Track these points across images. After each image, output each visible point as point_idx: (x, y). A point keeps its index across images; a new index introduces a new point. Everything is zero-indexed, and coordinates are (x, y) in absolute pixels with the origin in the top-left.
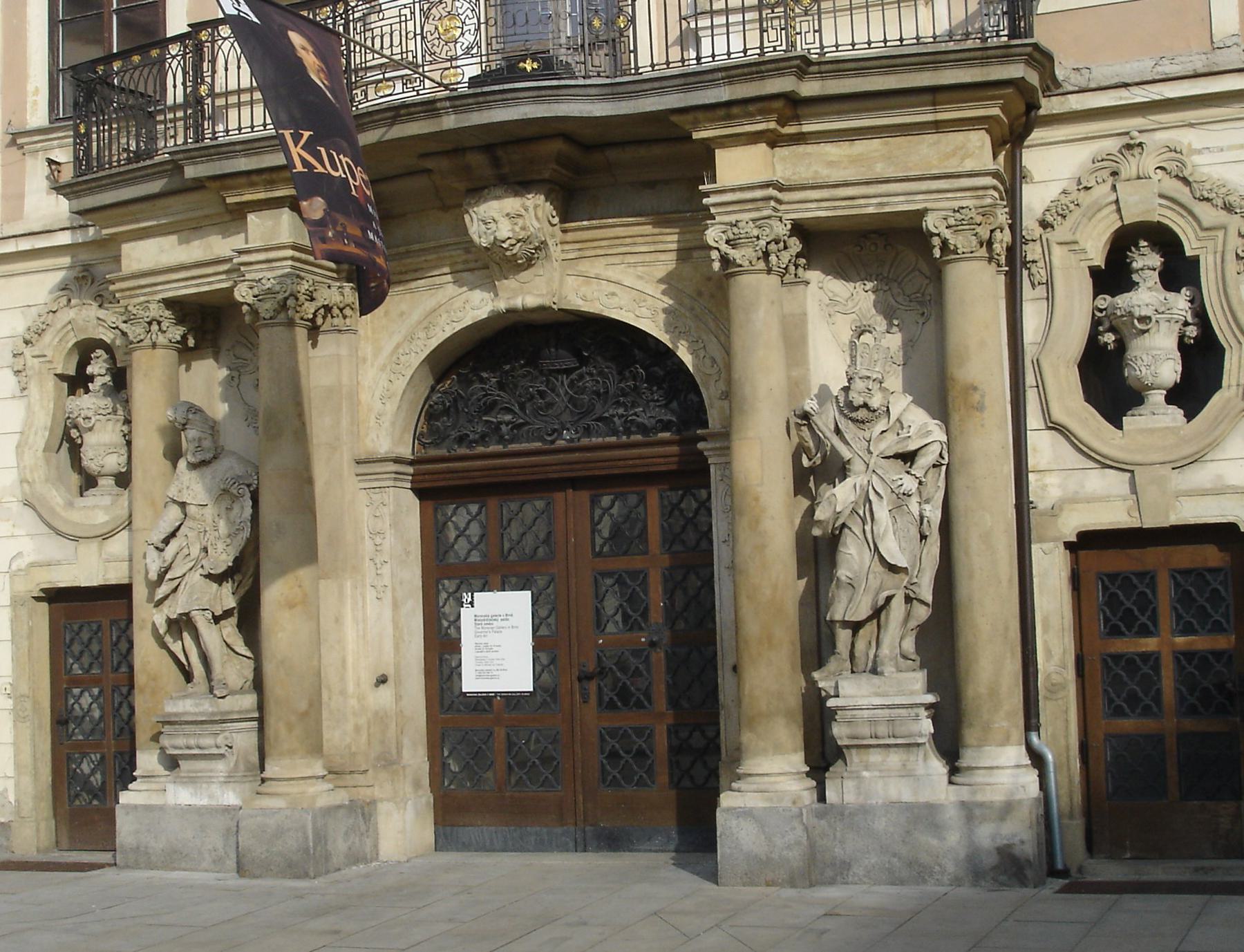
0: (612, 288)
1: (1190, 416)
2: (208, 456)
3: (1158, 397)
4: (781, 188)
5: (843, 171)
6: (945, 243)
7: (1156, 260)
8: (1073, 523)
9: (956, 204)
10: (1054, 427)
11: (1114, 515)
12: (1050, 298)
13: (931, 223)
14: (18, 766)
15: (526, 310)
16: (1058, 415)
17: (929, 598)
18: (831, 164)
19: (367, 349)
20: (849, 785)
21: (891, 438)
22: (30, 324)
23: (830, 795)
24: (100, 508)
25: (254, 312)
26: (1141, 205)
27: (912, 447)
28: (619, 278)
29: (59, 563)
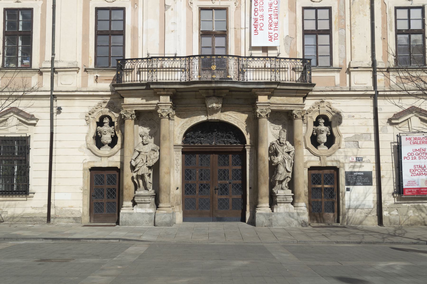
0: (230, 117)
1: (328, 149)
2: (147, 143)
3: (323, 144)
4: (271, 104)
5: (280, 102)
6: (296, 116)
7: (323, 121)
9: (299, 109)
10: (307, 148)
12: (307, 126)
13: (294, 112)
14: (83, 205)
15: (214, 120)
16: (308, 146)
17: (291, 177)
18: (277, 100)
19: (176, 124)
20: (278, 209)
21: (287, 149)
22: (90, 110)
23: (275, 210)
24: (106, 150)
25: (162, 116)
26: (323, 112)
27: (290, 150)
29: (96, 162)
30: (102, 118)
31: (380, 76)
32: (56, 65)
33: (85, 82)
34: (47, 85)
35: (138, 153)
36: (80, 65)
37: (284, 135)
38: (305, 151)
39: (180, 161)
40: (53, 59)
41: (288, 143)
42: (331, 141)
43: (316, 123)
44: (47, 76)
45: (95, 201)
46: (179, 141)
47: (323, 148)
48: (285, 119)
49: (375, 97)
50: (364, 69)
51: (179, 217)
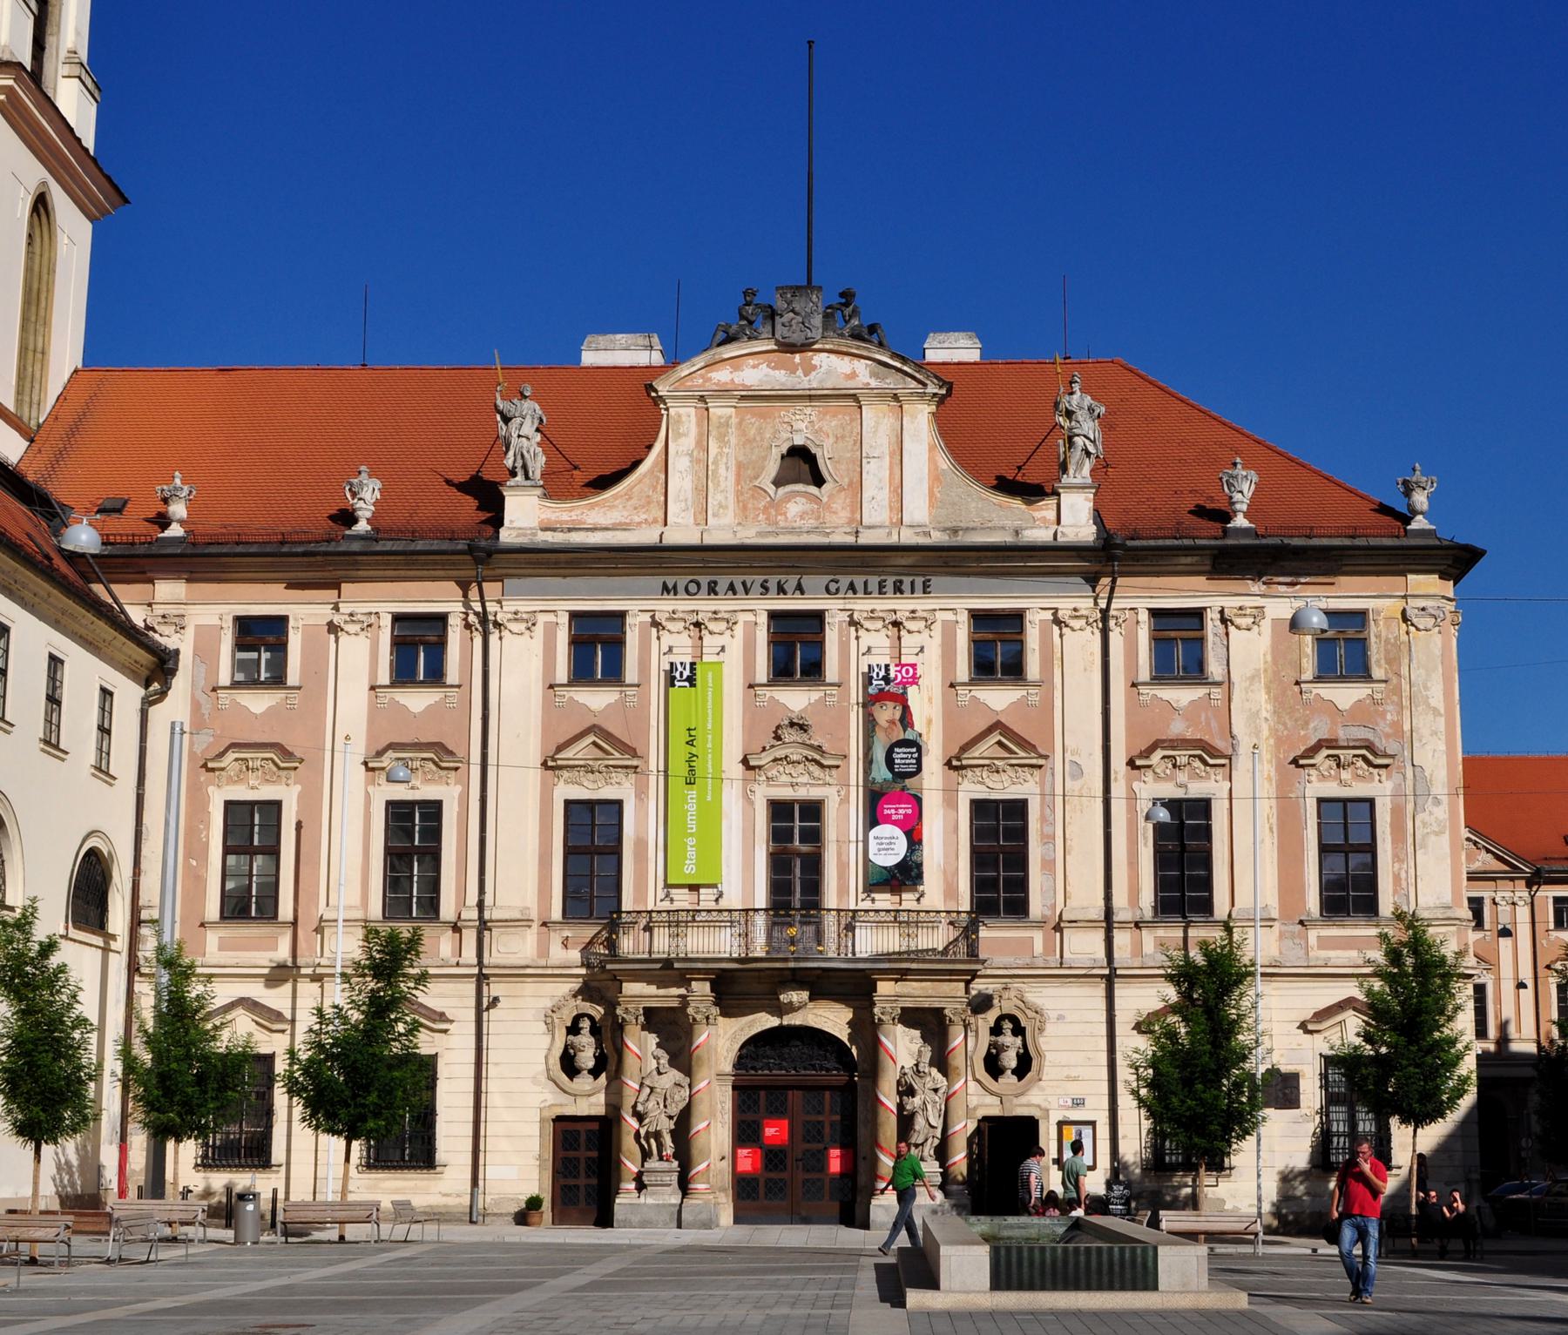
1: (1020, 1079)
8: (981, 1113)
11: (995, 1111)
19: (721, 1031)
24: (584, 1082)
26: (1008, 1007)
28: (833, 1019)
30: (577, 1019)
31: (1121, 939)
32: (487, 916)
33: (543, 950)
34: (470, 954)
35: (648, 1090)
36: (534, 915)
37: (927, 1053)
38: (972, 1084)
39: (729, 1105)
40: (481, 905)
41: (934, 1071)
42: (1024, 1065)
43: (996, 1030)
44: (470, 937)
45: (562, 1181)
46: (727, 1067)
47: (1009, 1079)
48: (931, 1024)
49: (1110, 980)
50: (1091, 923)
51: (726, 1216)
